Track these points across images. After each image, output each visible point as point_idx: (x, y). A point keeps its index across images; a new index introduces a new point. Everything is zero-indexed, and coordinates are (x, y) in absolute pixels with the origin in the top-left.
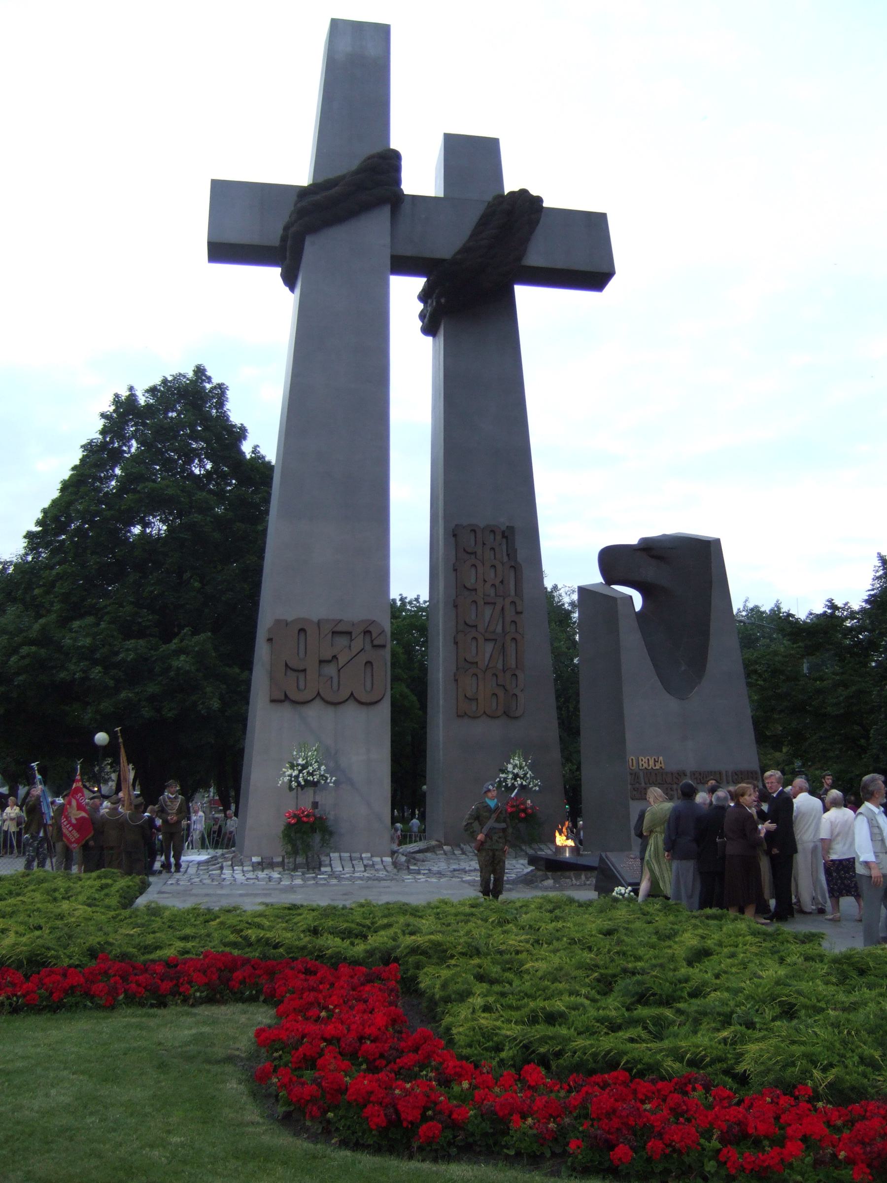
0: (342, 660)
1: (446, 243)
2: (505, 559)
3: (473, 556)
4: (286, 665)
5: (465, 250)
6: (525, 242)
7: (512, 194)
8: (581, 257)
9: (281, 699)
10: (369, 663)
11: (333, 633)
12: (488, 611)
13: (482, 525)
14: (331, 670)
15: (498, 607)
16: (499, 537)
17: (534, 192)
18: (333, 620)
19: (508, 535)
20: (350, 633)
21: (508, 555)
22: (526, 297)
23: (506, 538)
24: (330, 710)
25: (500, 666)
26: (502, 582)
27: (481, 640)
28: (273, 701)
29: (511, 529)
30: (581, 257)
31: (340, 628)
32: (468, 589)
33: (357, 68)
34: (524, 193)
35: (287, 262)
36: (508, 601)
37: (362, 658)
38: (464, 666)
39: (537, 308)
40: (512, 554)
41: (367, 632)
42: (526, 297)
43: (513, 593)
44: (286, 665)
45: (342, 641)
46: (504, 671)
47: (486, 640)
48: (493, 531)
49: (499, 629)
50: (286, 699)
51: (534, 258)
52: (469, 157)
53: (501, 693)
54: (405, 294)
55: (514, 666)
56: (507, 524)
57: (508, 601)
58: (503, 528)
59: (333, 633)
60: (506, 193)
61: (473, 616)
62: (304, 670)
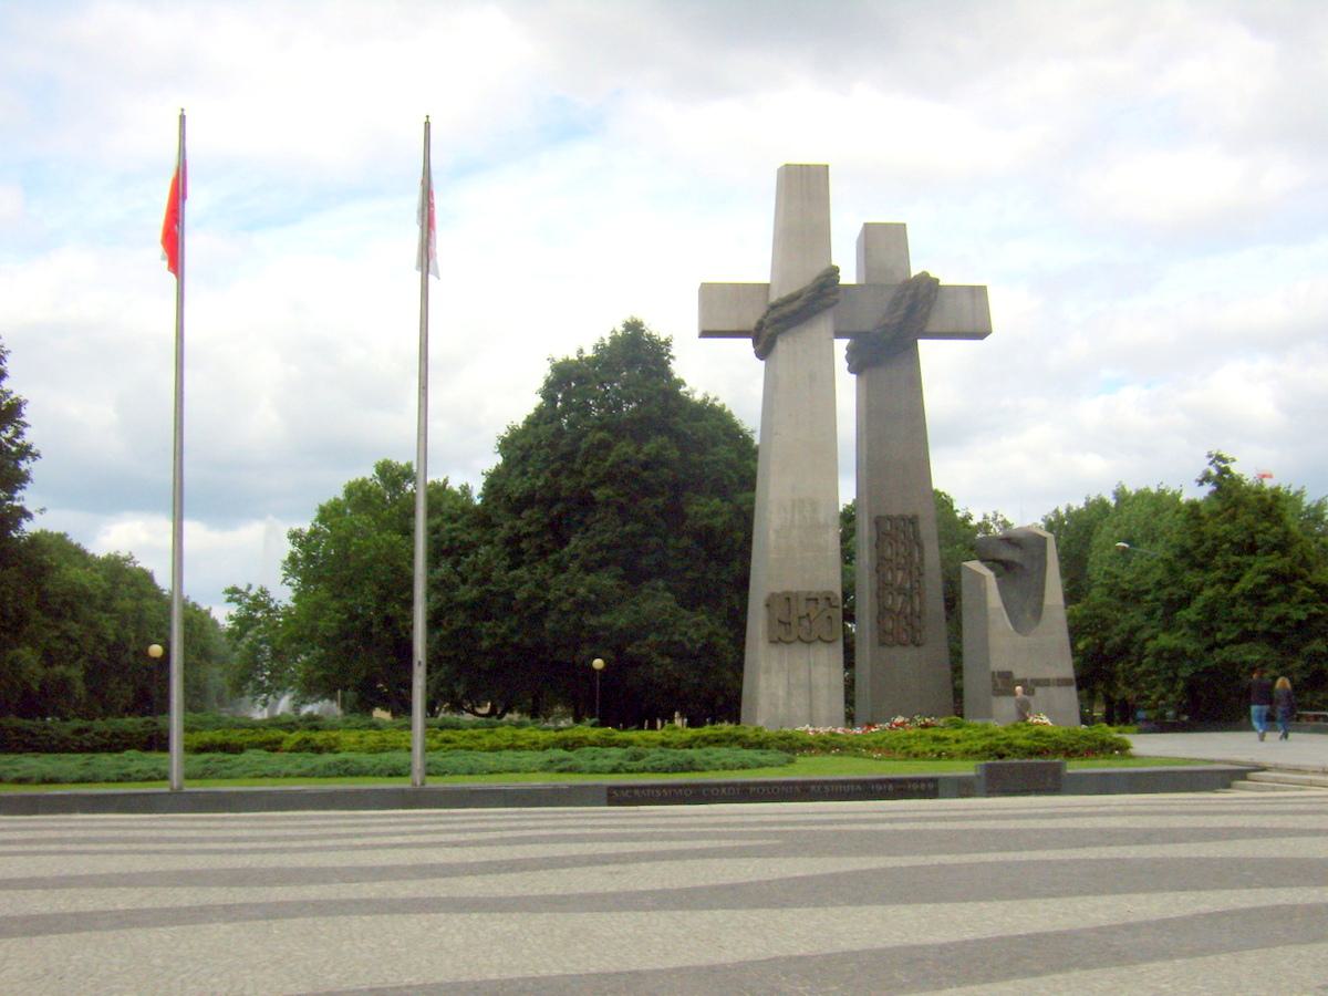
6: (926, 317)
7: (915, 277)
8: (964, 316)
9: (775, 641)
10: (829, 617)
12: (900, 574)
14: (805, 623)
17: (932, 275)
20: (816, 600)
22: (924, 346)
25: (908, 610)
27: (895, 593)
28: (772, 642)
30: (964, 316)
33: (804, 190)
34: (924, 277)
35: (760, 346)
38: (883, 612)
39: (931, 352)
40: (916, 533)
41: (828, 599)
42: (924, 346)
43: (917, 560)
44: (780, 621)
46: (912, 614)
49: (908, 586)
50: (780, 640)
51: (932, 327)
52: (882, 241)
53: (909, 628)
54: (841, 346)
60: (912, 276)
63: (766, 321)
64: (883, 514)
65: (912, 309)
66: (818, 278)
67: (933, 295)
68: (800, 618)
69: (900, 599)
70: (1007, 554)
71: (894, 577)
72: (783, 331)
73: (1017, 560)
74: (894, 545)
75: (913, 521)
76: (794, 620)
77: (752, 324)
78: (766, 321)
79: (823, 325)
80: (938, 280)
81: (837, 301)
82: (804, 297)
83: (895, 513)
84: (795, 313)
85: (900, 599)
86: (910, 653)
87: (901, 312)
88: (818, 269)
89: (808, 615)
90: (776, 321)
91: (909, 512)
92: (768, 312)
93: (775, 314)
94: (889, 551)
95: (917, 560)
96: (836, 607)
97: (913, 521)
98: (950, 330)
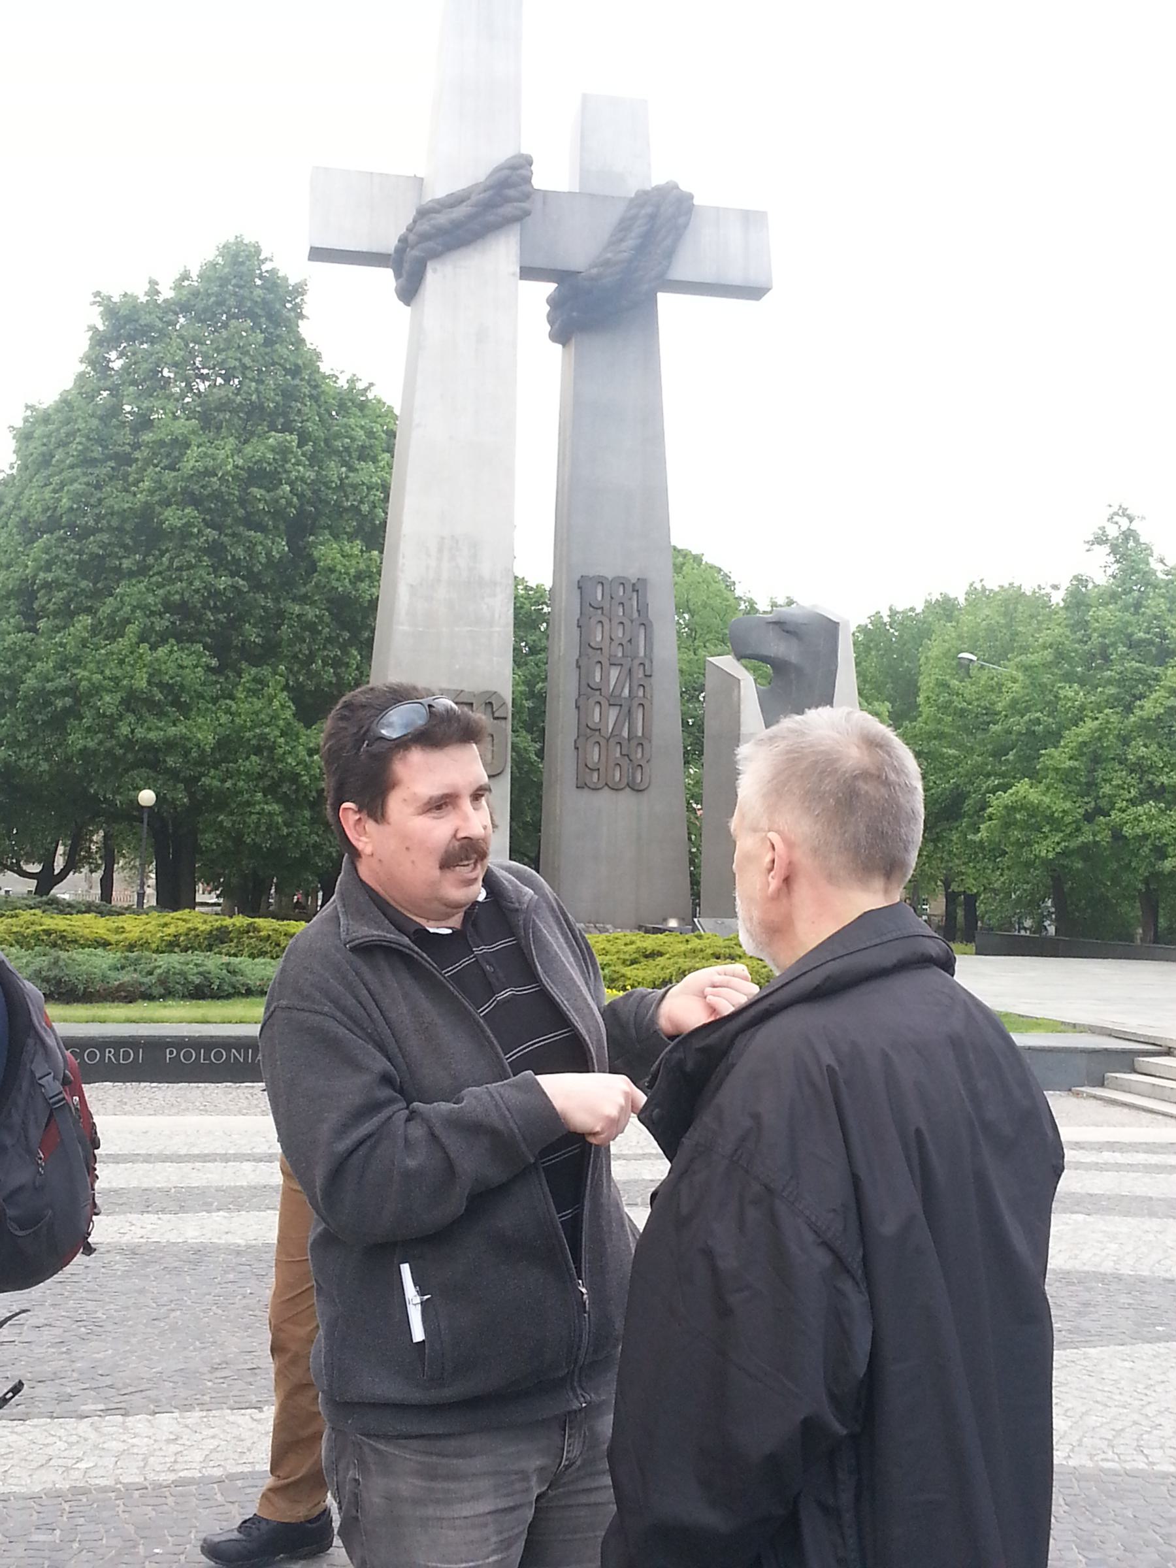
1: (581, 249)
2: (635, 615)
3: (600, 611)
6: (670, 254)
13: (609, 574)
16: (629, 588)
17: (685, 187)
21: (638, 611)
26: (630, 641)
27: (605, 703)
35: (400, 280)
36: (636, 662)
38: (587, 732)
40: (643, 610)
43: (642, 654)
49: (626, 692)
51: (681, 271)
55: (640, 734)
57: (636, 662)
58: (634, 581)
61: (598, 679)
63: (412, 238)
64: (592, 573)
65: (648, 239)
66: (499, 169)
67: (681, 220)
69: (613, 713)
70: (778, 647)
71: (605, 677)
72: (435, 255)
73: (794, 659)
74: (607, 627)
75: (638, 587)
77: (389, 245)
78: (412, 238)
79: (502, 254)
80: (691, 197)
81: (527, 213)
82: (474, 198)
84: (457, 225)
85: (613, 713)
86: (626, 799)
87: (630, 243)
88: (500, 154)
90: (424, 237)
91: (632, 574)
92: (415, 222)
93: (424, 226)
95: (642, 654)
97: (638, 587)
98: (709, 279)
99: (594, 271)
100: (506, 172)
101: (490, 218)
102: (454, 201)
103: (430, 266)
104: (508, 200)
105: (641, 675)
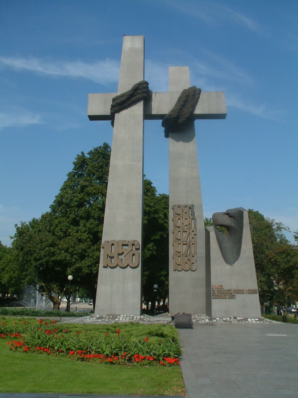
0: (125, 253)
4: (108, 255)
5: (173, 111)
11: (122, 245)
14: (122, 257)
15: (188, 233)
18: (123, 241)
19: (191, 207)
21: (191, 215)
23: (190, 209)
24: (122, 269)
26: (189, 224)
27: (182, 244)
29: (193, 206)
31: (125, 243)
32: (177, 227)
36: (191, 230)
37: (132, 253)
40: (193, 214)
43: (193, 227)
44: (108, 255)
45: (126, 247)
47: (184, 244)
48: (186, 207)
55: (193, 253)
56: (191, 204)
57: (191, 230)
59: (123, 245)
62: (113, 257)
68: (119, 254)
76: (116, 256)
83: (182, 203)
89: (123, 253)
91: (190, 203)
94: (179, 224)
95: (193, 227)
96: (138, 249)
99: (171, 113)
100: (137, 86)
101: (133, 99)
102: (122, 96)
103: (116, 115)
104: (138, 94)
105: (193, 235)
